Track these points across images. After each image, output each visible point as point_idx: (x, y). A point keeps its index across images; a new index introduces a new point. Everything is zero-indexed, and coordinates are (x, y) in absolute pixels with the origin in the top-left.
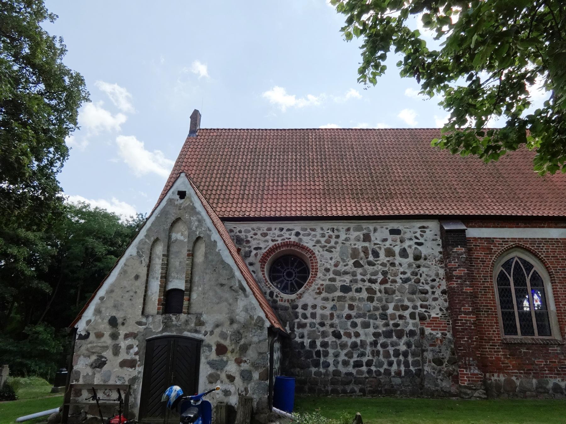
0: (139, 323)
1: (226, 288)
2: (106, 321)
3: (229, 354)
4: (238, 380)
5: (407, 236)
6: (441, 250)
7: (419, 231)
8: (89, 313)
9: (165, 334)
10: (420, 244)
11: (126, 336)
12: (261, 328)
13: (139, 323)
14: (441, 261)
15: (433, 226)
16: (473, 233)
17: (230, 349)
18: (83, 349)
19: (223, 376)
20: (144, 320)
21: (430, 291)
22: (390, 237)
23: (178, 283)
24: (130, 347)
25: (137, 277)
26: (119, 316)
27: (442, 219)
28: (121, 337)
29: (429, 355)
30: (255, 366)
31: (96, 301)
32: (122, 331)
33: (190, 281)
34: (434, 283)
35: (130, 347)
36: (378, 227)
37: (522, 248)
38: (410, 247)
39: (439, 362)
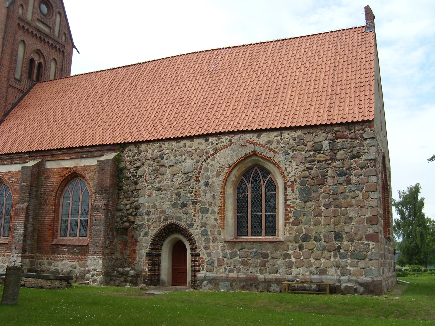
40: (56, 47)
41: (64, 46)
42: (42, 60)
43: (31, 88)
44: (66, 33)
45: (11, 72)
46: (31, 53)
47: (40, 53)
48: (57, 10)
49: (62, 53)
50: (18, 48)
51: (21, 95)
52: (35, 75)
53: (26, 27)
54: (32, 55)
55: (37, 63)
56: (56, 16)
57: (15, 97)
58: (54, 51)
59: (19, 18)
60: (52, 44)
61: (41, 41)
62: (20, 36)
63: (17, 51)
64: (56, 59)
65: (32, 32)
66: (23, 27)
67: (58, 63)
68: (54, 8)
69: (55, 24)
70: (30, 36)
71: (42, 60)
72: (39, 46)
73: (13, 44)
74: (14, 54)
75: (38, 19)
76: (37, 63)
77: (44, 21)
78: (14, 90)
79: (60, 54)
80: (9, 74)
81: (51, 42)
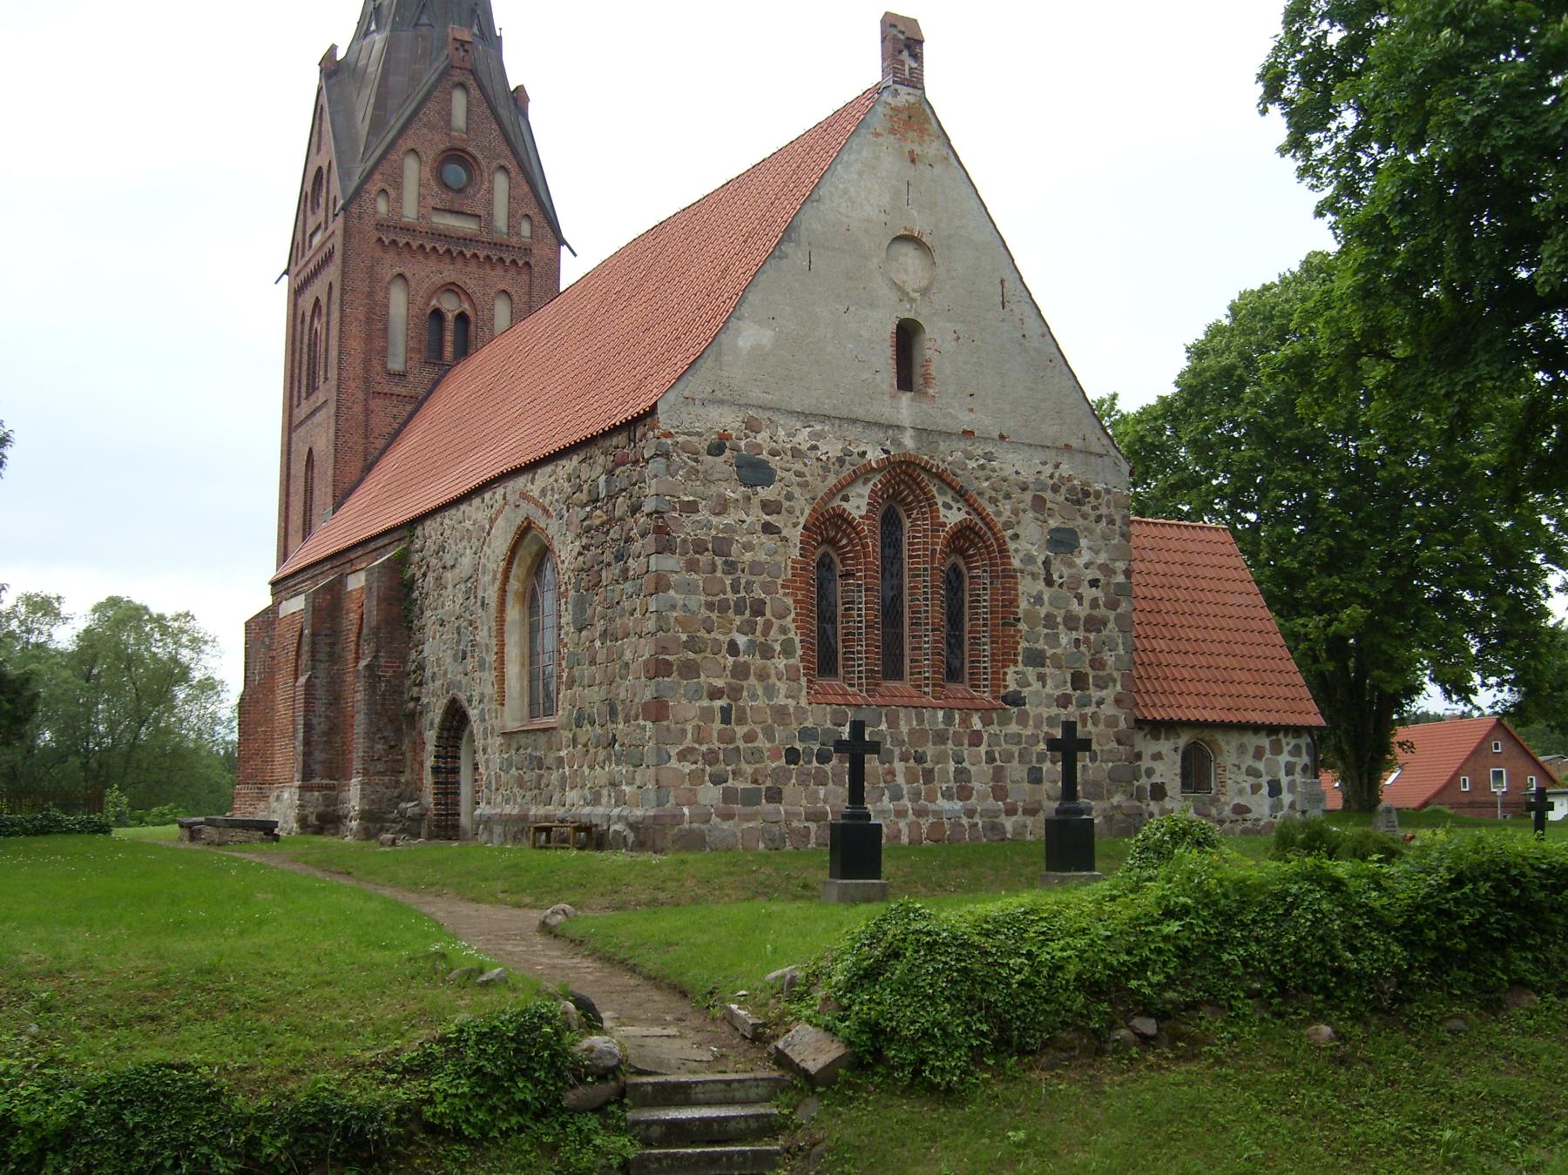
40: (501, 260)
41: (527, 251)
42: (466, 306)
43: (436, 383)
44: (531, 213)
45: (375, 362)
46: (430, 299)
47: (460, 292)
48: (495, 164)
49: (525, 270)
50: (387, 298)
51: (409, 408)
52: (449, 350)
53: (402, 241)
54: (434, 302)
55: (450, 316)
56: (491, 182)
57: (395, 417)
58: (499, 271)
59: (380, 226)
60: (488, 258)
61: (453, 259)
62: (389, 265)
63: (387, 307)
64: (509, 290)
65: (422, 247)
66: (394, 242)
67: (516, 298)
68: (483, 163)
69: (490, 202)
70: (420, 257)
71: (466, 306)
72: (450, 273)
73: (370, 294)
74: (377, 319)
75: (434, 209)
76: (450, 316)
77: (456, 208)
78: (387, 402)
79: (519, 273)
80: (367, 370)
81: (482, 254)
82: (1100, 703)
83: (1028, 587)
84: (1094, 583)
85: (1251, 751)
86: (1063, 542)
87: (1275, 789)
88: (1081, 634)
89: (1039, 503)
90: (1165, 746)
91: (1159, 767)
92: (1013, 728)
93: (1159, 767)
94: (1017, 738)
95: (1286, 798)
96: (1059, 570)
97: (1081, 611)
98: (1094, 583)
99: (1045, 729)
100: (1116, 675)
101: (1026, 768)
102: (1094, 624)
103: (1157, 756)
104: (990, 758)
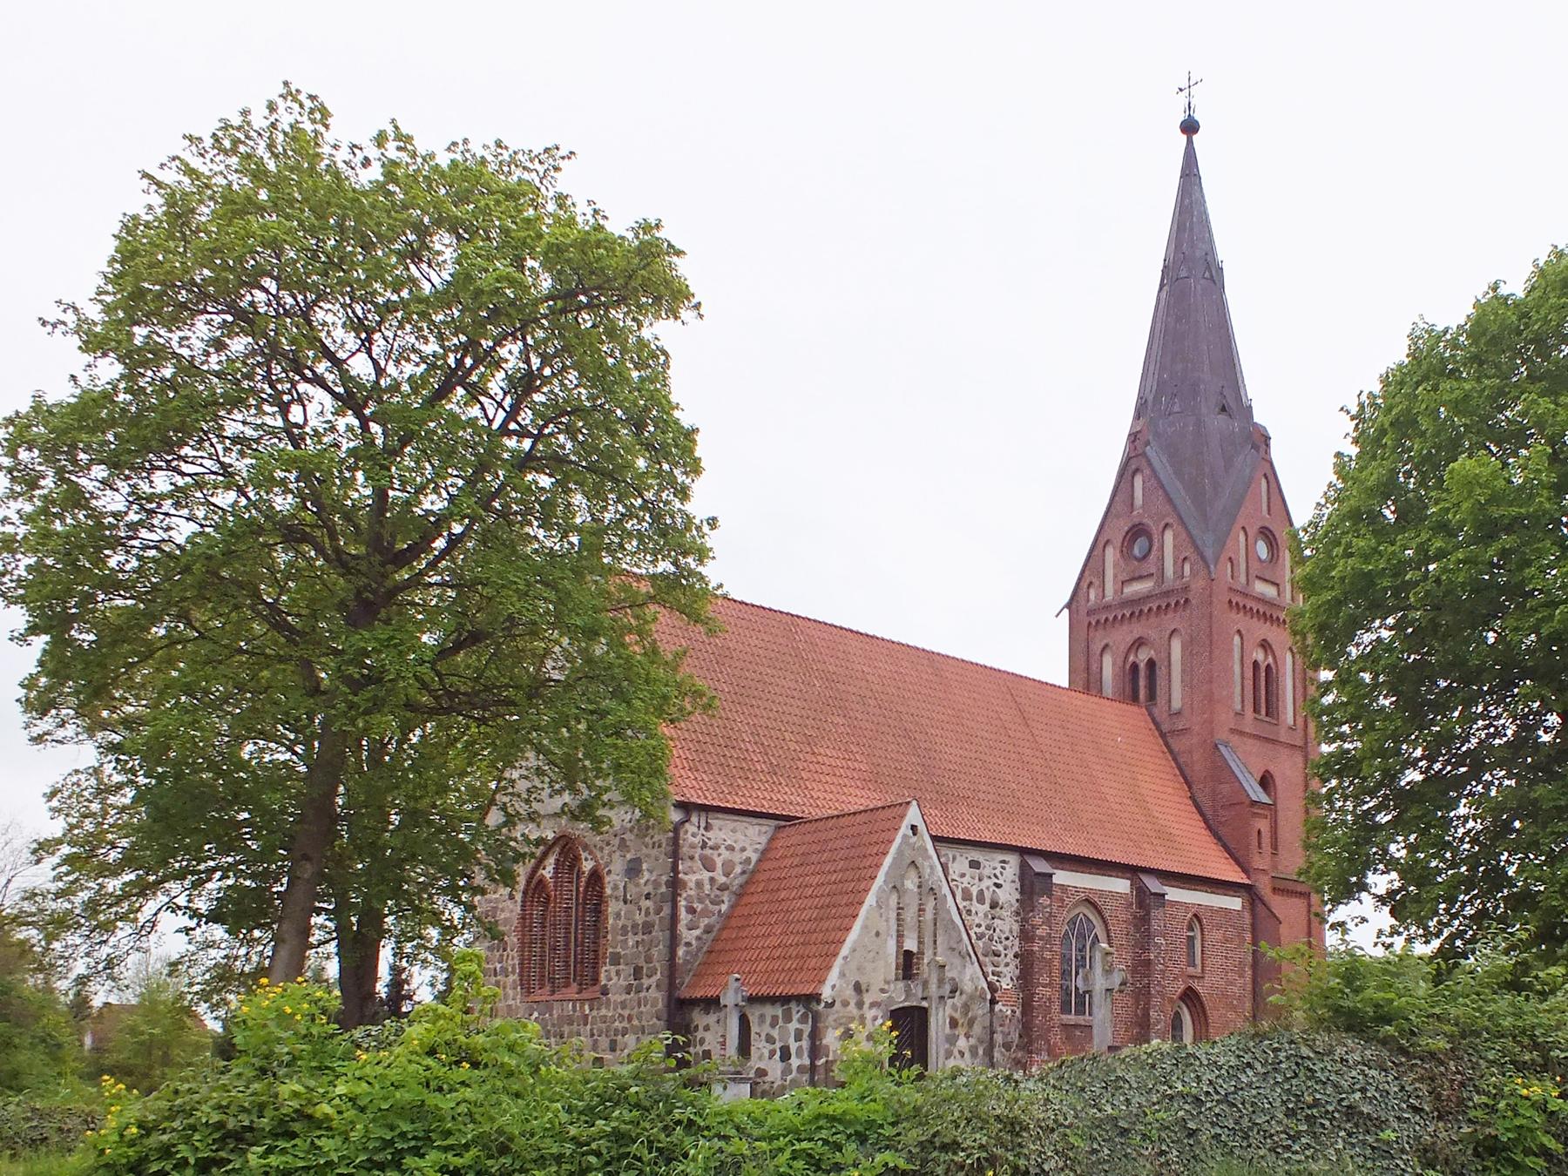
0: (883, 991)
1: (956, 953)
2: (851, 986)
3: (960, 1028)
4: (967, 1055)
5: (987, 872)
6: (1018, 897)
7: (999, 866)
8: (833, 976)
9: (906, 1004)
10: (998, 886)
11: (873, 1005)
12: (985, 999)
13: (883, 991)
14: (1018, 914)
15: (1013, 860)
16: (1061, 877)
17: (960, 1022)
18: (831, 1019)
19: (956, 1053)
20: (886, 987)
21: (1003, 952)
22: (969, 871)
23: (911, 945)
24: (875, 1018)
25: (878, 934)
26: (863, 981)
27: (1023, 852)
28: (866, 1006)
29: (998, 1038)
30: (981, 1041)
31: (839, 961)
32: (868, 999)
33: (920, 943)
34: (1007, 942)
35: (875, 1018)
36: (958, 855)
37: (1090, 903)
38: (988, 888)
39: (1007, 1046)
82: (648, 989)
83: (613, 907)
84: (648, 896)
85: (768, 1020)
86: (633, 870)
87: (785, 1055)
88: (639, 938)
89: (623, 845)
90: (711, 1019)
91: (708, 1036)
92: (603, 1012)
93: (708, 1036)
94: (604, 1019)
95: (795, 1062)
96: (632, 891)
97: (640, 918)
98: (648, 896)
99: (619, 1011)
100: (658, 965)
101: (608, 1040)
102: (648, 928)
103: (707, 1028)
104: (592, 1035)
